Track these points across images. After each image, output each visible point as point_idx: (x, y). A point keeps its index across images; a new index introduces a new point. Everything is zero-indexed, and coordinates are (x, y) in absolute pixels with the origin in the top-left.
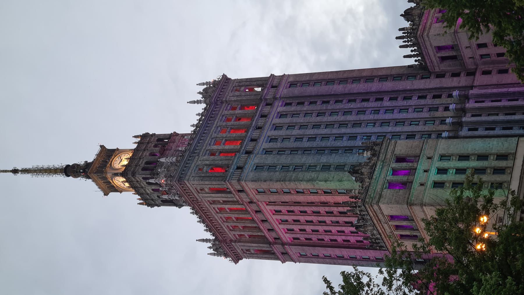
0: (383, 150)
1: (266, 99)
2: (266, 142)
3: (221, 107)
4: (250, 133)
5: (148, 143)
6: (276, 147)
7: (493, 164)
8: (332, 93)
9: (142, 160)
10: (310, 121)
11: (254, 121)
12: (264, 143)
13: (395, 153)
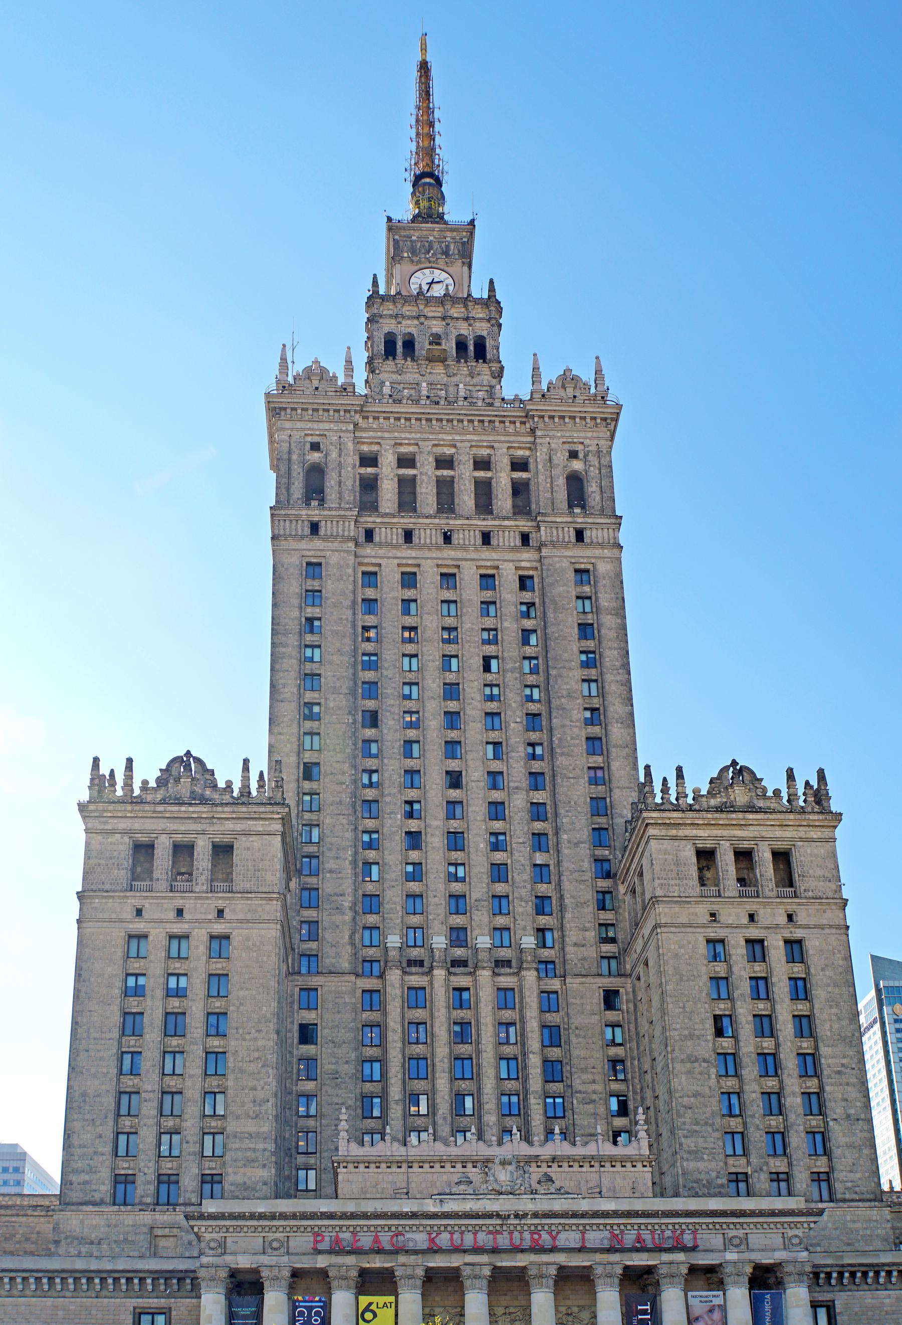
0: (244, 809)
1: (538, 527)
2: (399, 565)
3: (517, 434)
4: (428, 521)
5: (467, 319)
6: (385, 589)
7: (195, 1047)
8: (553, 672)
9: (416, 322)
10: (466, 646)
11: (466, 522)
12: (396, 561)
13: (244, 838)
